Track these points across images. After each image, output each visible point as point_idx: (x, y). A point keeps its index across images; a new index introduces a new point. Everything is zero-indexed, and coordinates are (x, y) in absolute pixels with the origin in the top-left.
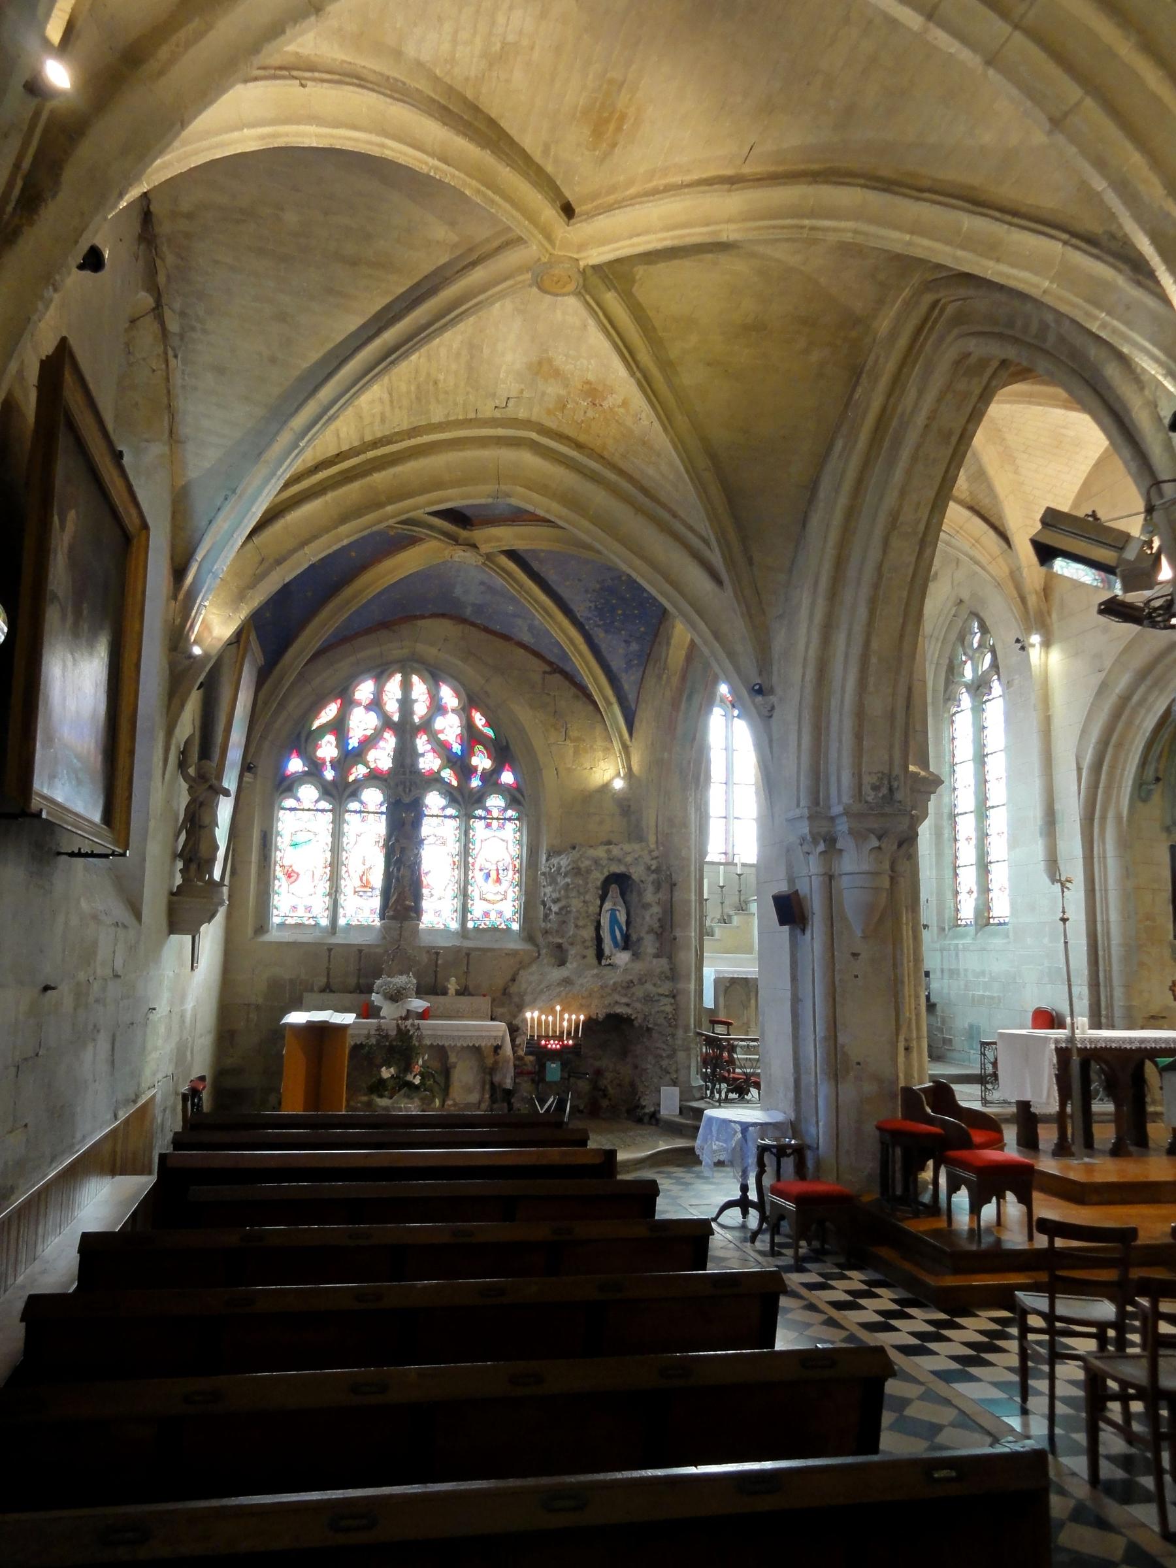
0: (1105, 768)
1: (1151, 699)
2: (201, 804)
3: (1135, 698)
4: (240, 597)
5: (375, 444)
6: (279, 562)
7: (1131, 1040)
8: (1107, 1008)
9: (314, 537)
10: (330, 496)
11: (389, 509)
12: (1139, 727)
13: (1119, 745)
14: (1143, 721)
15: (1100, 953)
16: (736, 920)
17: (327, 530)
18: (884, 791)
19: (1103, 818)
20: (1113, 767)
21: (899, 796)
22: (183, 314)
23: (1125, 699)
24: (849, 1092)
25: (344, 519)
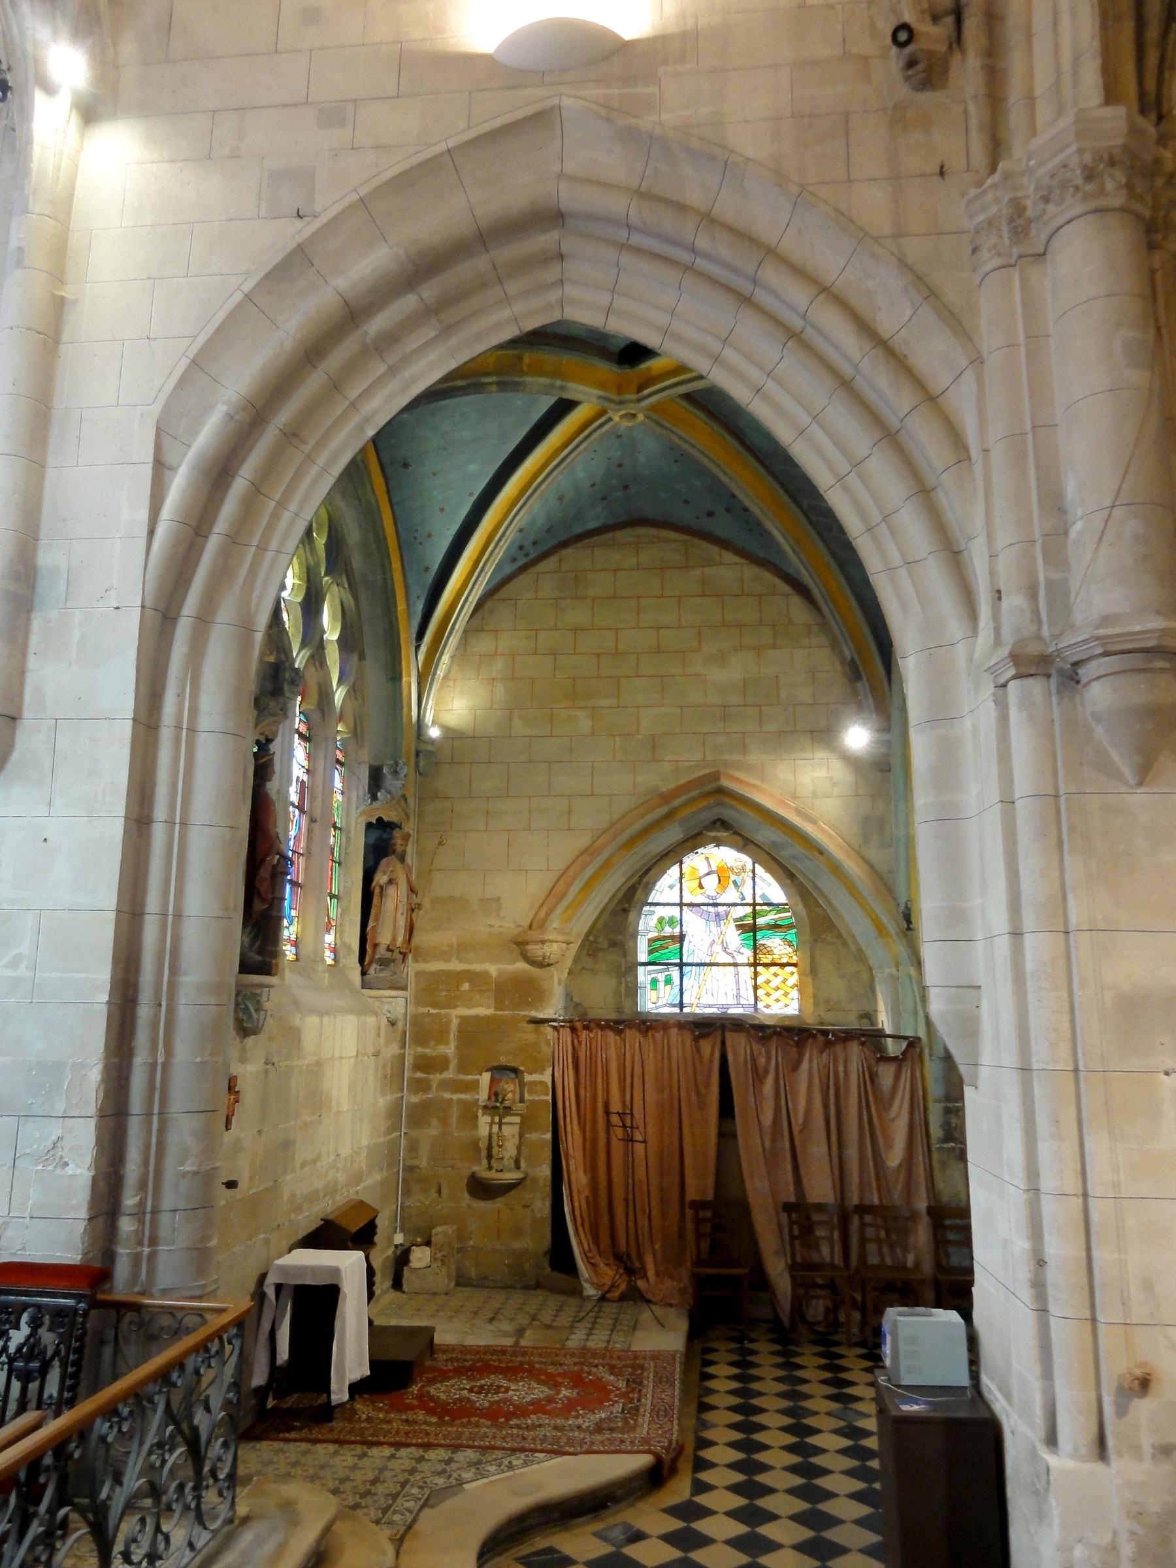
0: (239, 485)
1: (411, 344)
3: (378, 324)
8: (142, 1185)
12: (354, 405)
13: (292, 436)
14: (366, 394)
15: (144, 1012)
19: (204, 620)
20: (257, 490)
23: (351, 315)
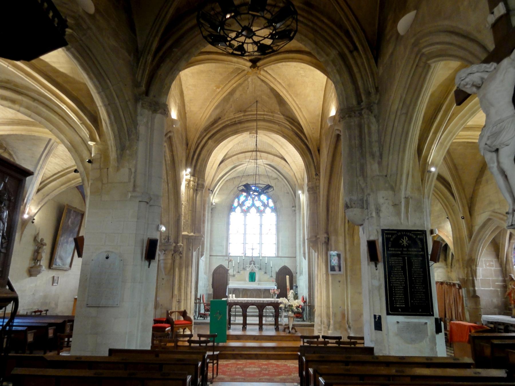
2: (40, 248)
4: (39, 204)
5: (67, 169)
6: (47, 195)
7: (244, 300)
9: (55, 190)
10: (58, 181)
11: (73, 182)
16: (242, 272)
17: (58, 188)
18: (167, 240)
21: (170, 241)
22: (13, 151)
24: (159, 311)
25: (62, 185)
